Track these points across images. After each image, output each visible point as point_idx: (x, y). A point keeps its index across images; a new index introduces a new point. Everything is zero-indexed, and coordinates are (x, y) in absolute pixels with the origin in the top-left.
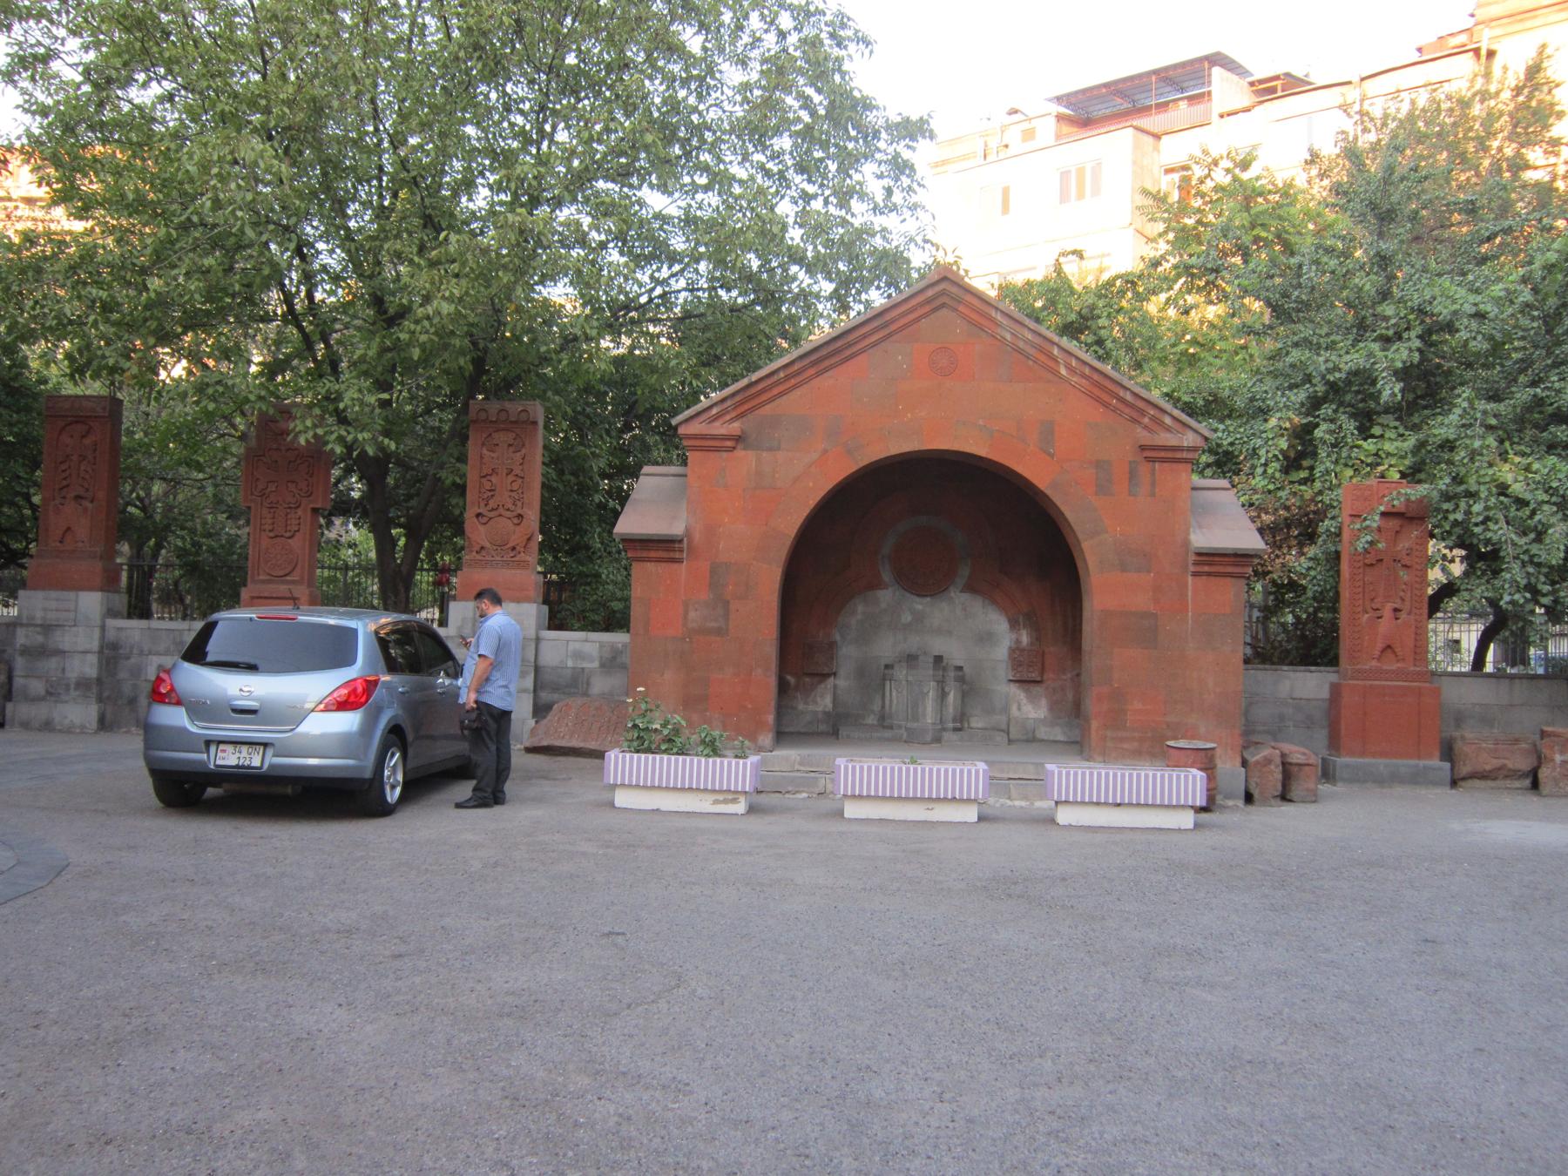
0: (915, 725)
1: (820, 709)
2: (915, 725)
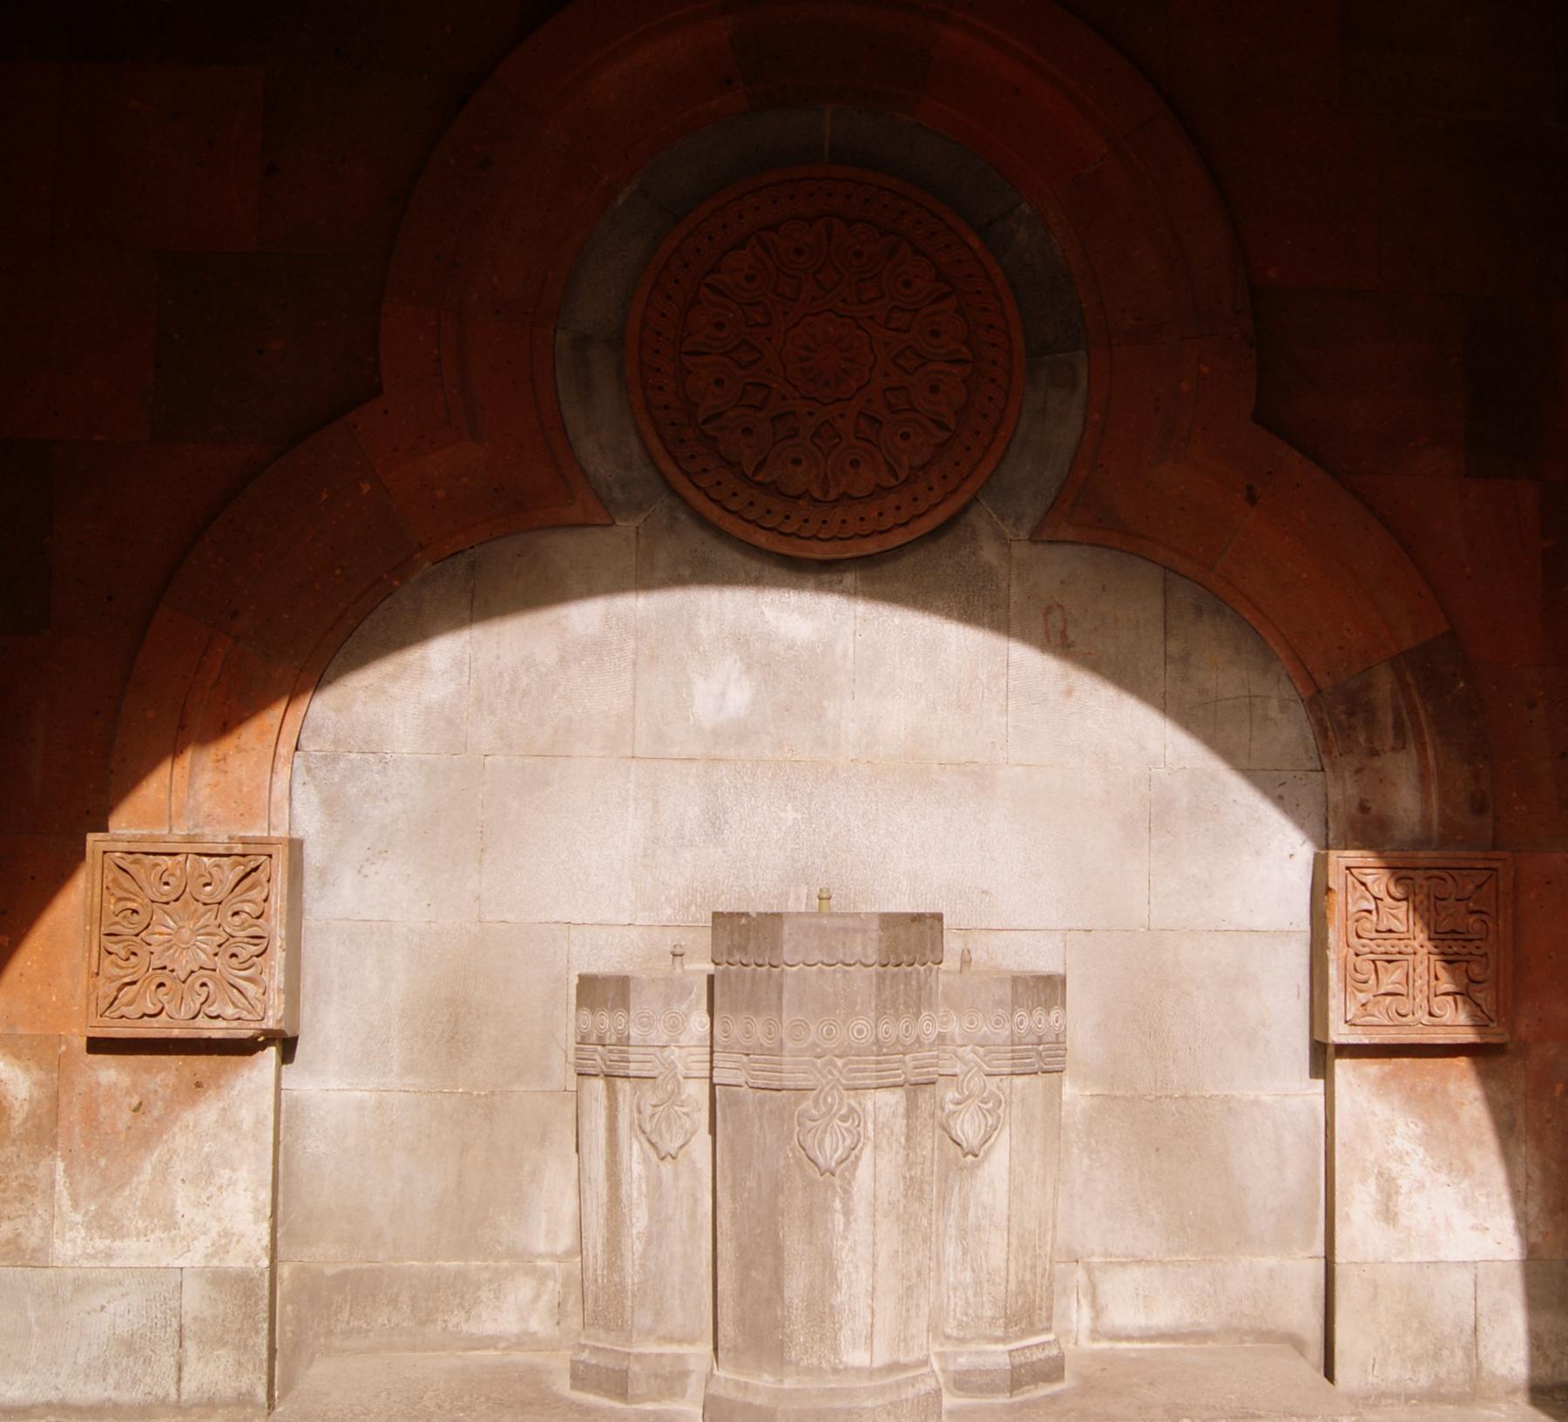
0: (763, 1384)
1: (195, 1258)
2: (763, 1384)
